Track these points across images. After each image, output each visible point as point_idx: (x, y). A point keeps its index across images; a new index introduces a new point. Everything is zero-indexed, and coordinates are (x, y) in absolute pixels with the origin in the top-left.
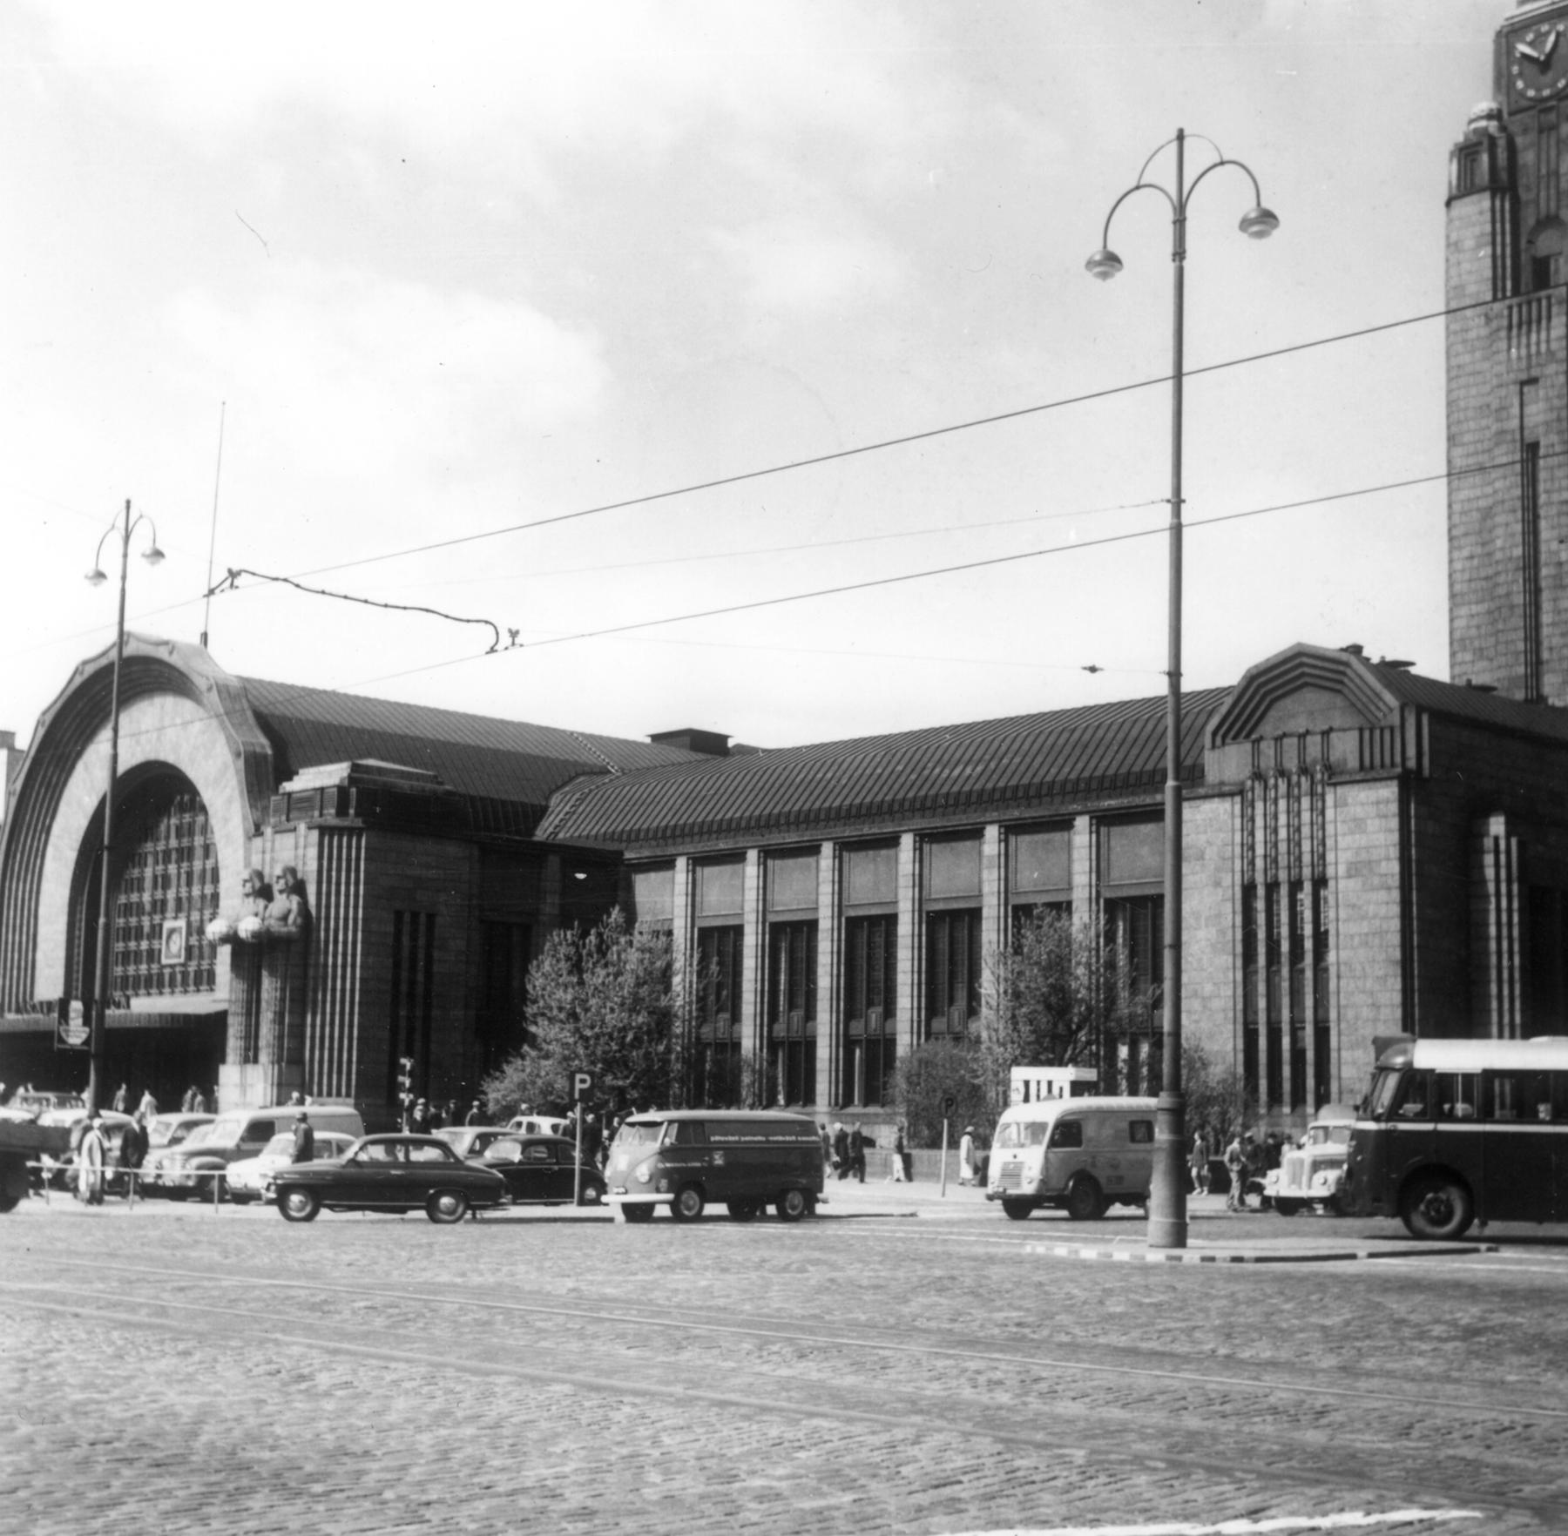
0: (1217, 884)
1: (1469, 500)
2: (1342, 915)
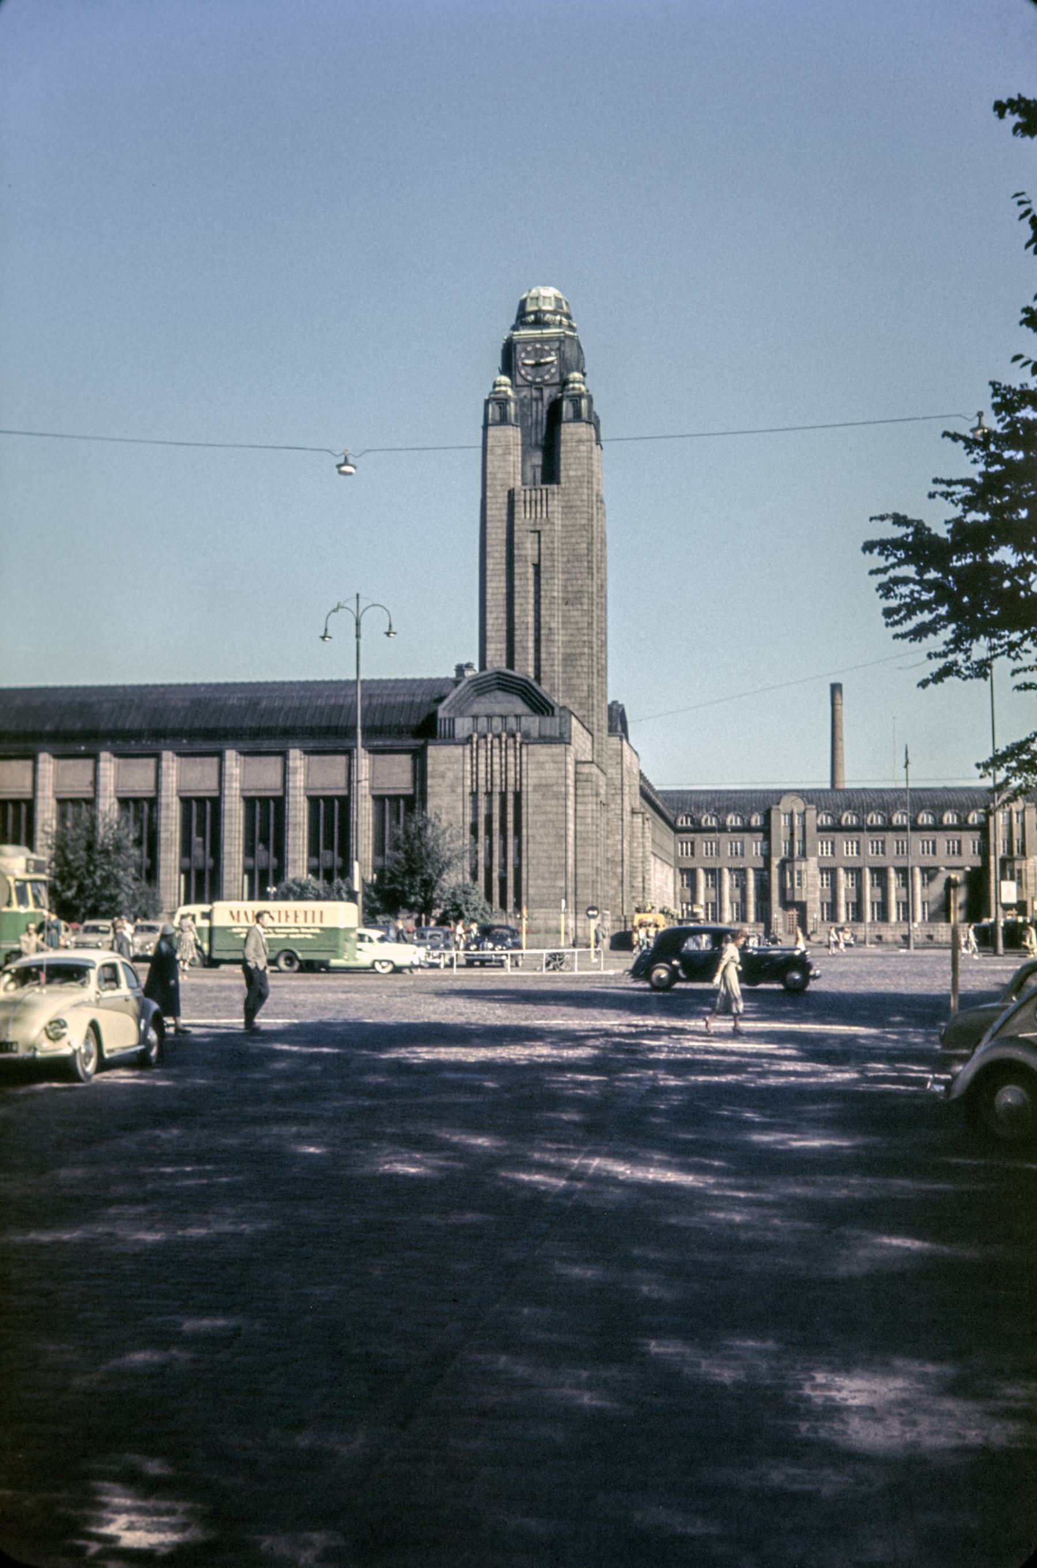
0: (453, 791)
1: (497, 588)
2: (530, 810)
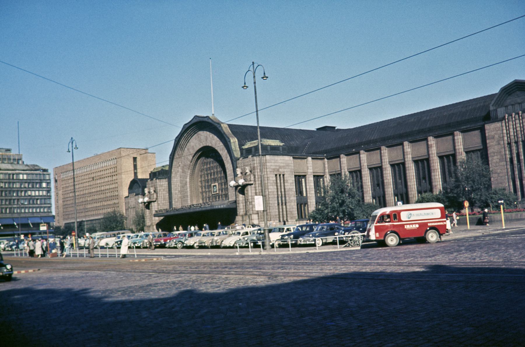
0: (499, 144)
